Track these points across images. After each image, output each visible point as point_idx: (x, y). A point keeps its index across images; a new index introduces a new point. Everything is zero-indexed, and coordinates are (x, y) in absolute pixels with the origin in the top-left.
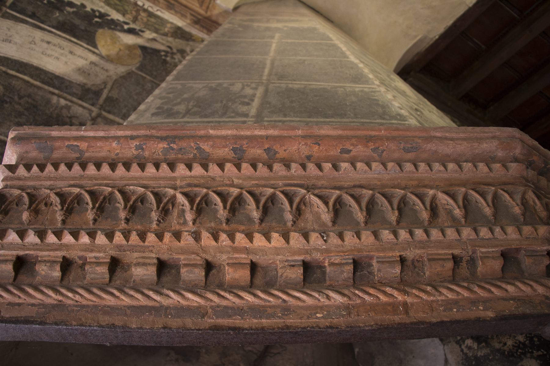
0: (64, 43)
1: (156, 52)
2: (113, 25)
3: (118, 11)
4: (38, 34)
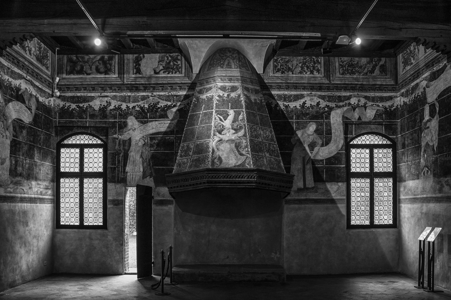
0: (162, 122)
1: (182, 108)
2: (169, 107)
3: (169, 101)
4: (157, 122)
